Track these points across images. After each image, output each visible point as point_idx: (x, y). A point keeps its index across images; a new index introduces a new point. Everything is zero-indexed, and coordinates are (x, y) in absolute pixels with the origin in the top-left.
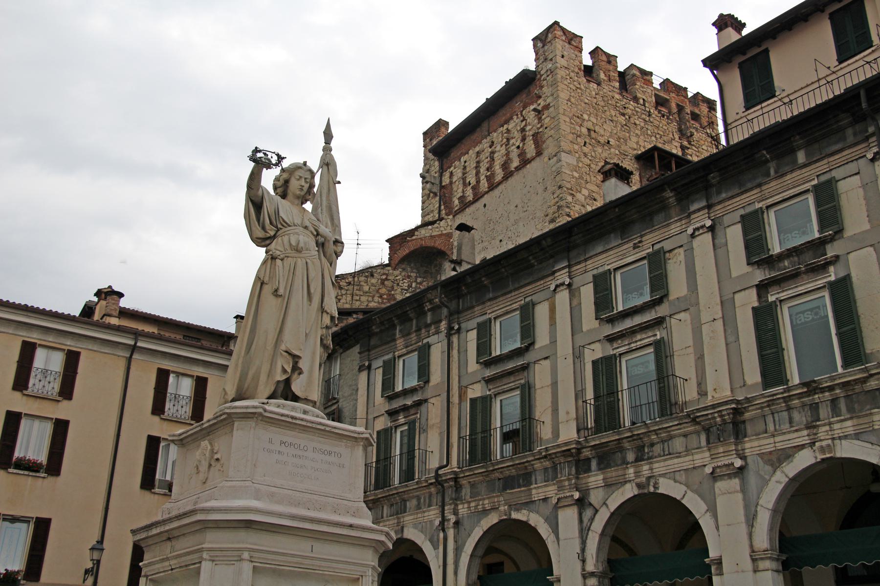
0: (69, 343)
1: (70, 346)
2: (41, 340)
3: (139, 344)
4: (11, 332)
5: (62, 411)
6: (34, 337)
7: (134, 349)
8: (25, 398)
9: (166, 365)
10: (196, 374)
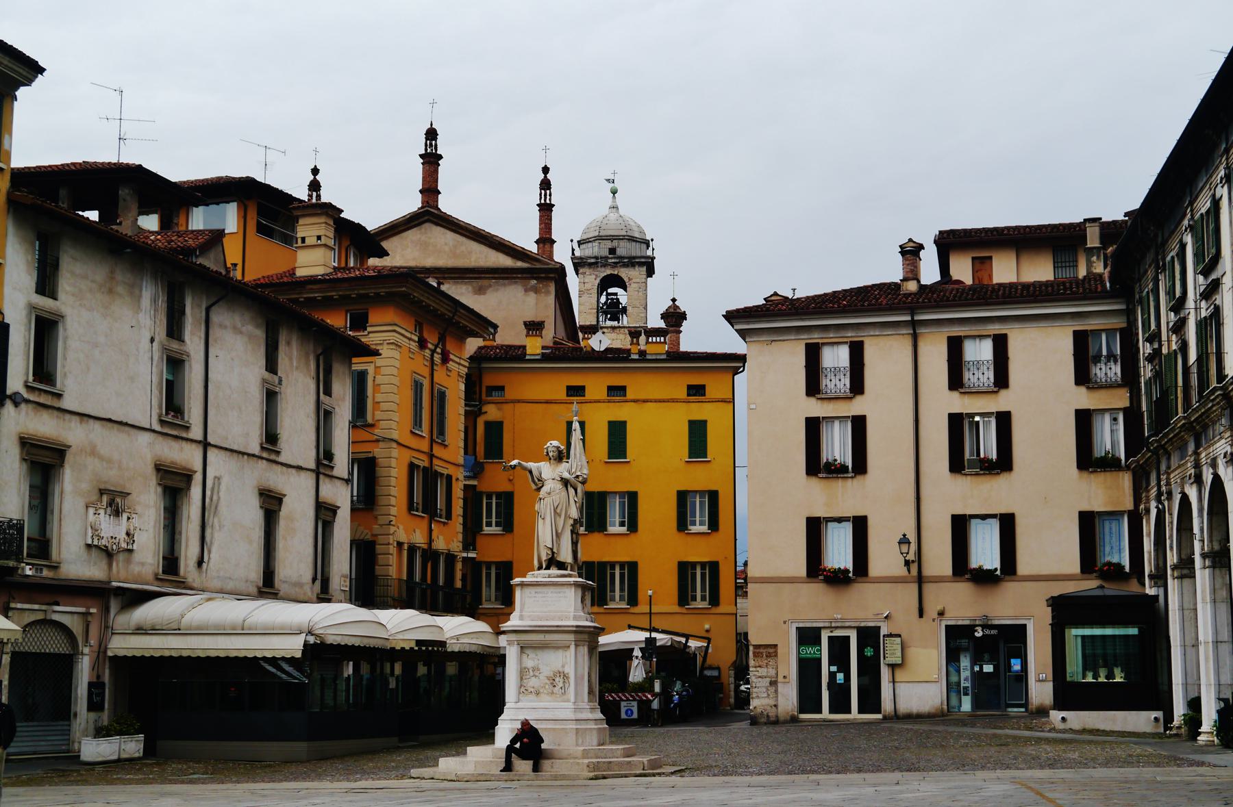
0: (850, 335)
1: (852, 337)
2: (822, 338)
3: (916, 318)
4: (793, 338)
5: (857, 407)
6: (815, 338)
7: (914, 324)
8: (819, 402)
9: (957, 331)
10: (992, 333)
